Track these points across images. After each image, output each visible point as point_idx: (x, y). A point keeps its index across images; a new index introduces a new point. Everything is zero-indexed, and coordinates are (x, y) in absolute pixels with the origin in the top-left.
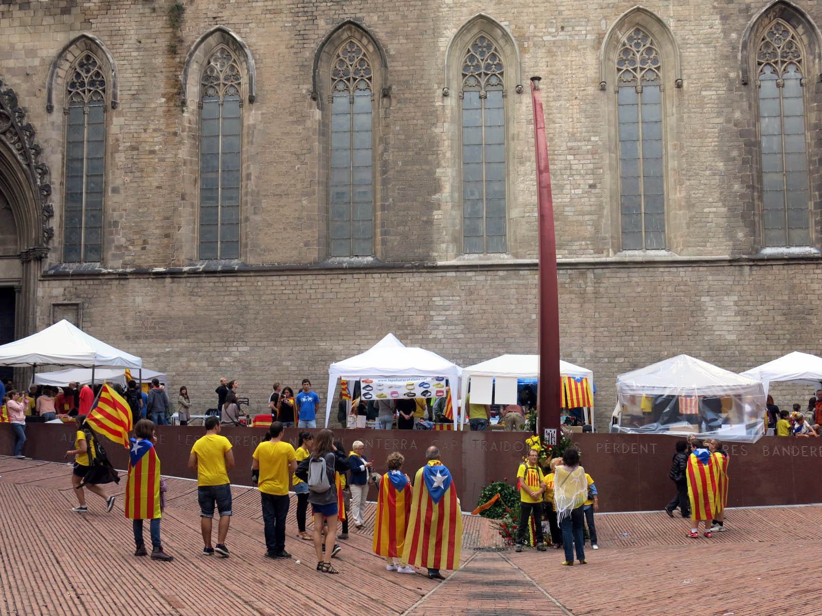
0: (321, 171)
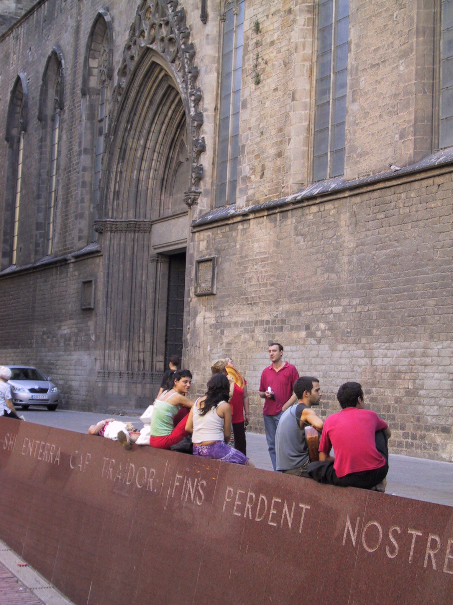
0: (422, 11)
